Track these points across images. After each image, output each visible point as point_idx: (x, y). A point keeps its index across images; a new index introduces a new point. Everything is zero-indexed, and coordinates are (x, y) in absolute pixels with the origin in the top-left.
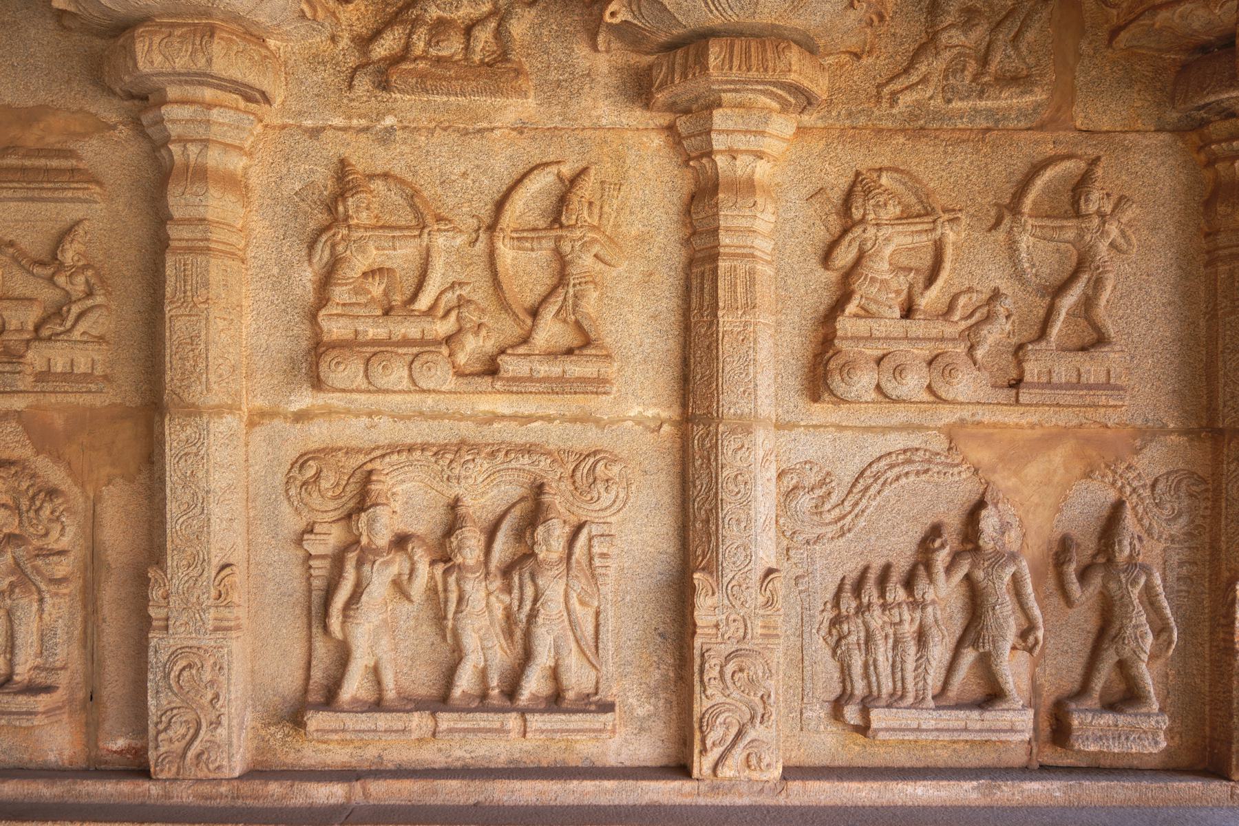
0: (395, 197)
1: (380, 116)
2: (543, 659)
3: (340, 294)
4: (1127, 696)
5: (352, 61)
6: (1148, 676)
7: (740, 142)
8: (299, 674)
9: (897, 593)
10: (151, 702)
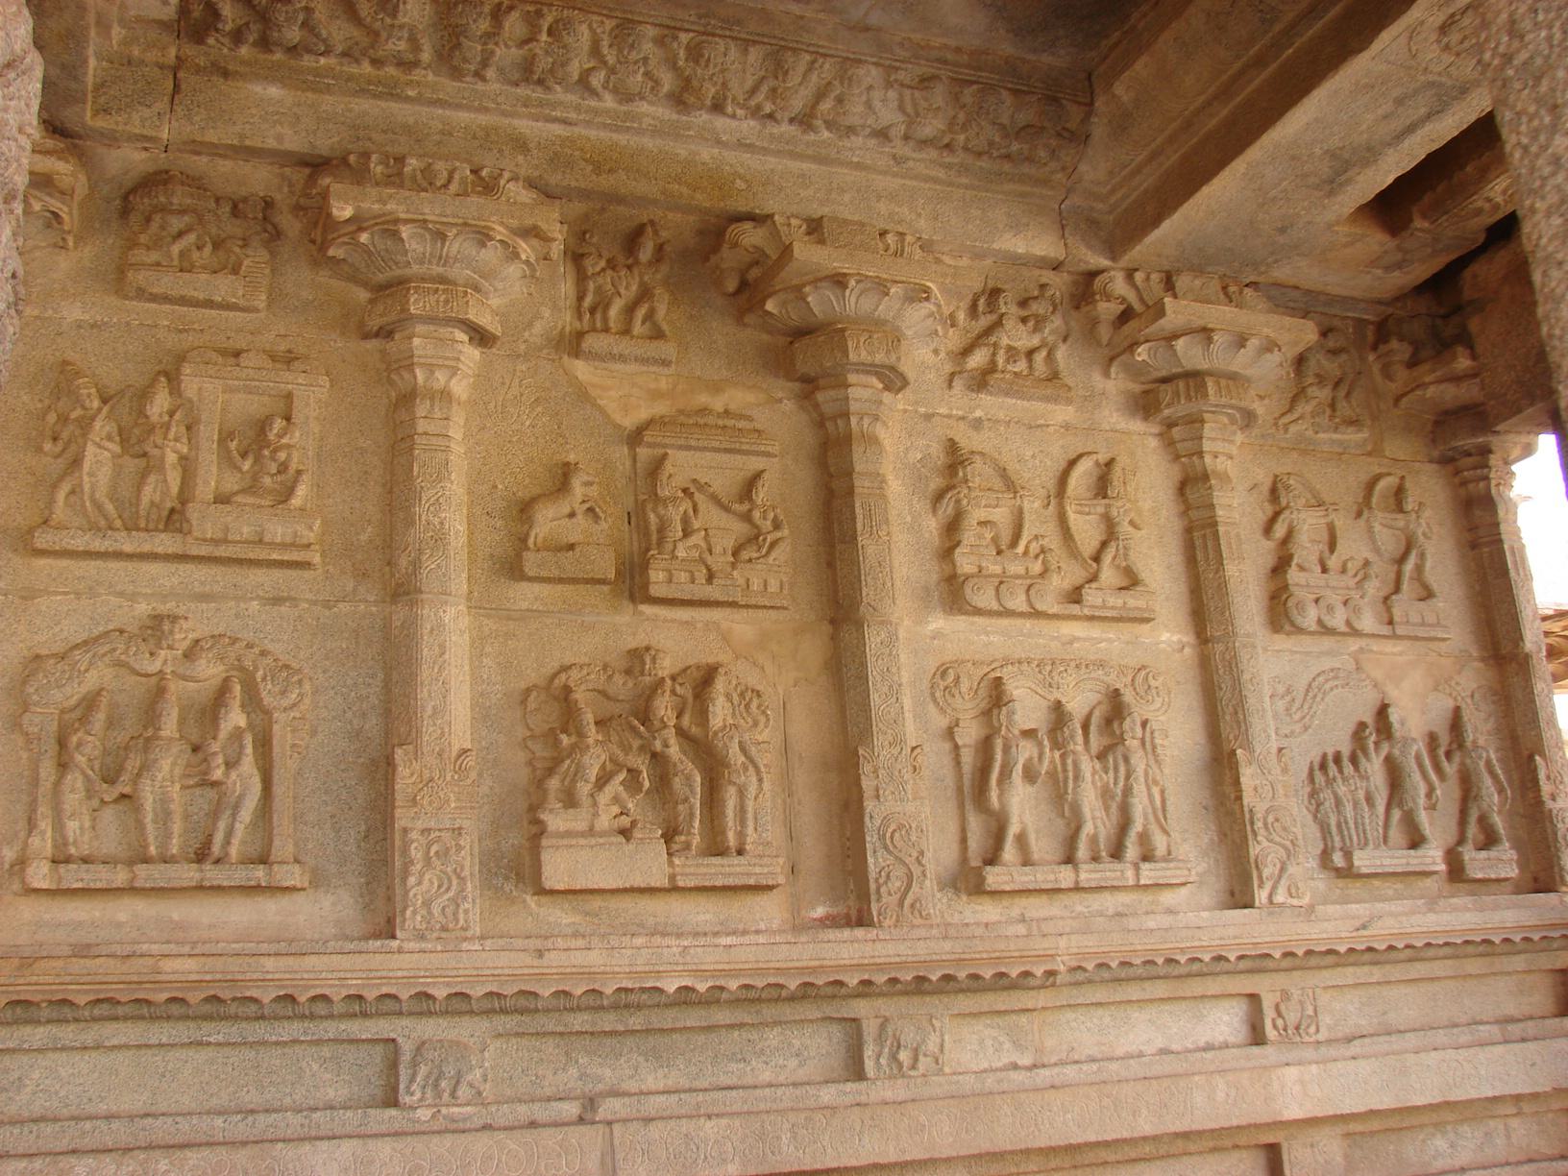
0: (988, 470)
1: (972, 410)
2: (1137, 827)
3: (969, 536)
4: (1489, 840)
5: (948, 368)
6: (1498, 821)
7: (1219, 447)
8: (955, 847)
9: (1348, 768)
10: (871, 860)
